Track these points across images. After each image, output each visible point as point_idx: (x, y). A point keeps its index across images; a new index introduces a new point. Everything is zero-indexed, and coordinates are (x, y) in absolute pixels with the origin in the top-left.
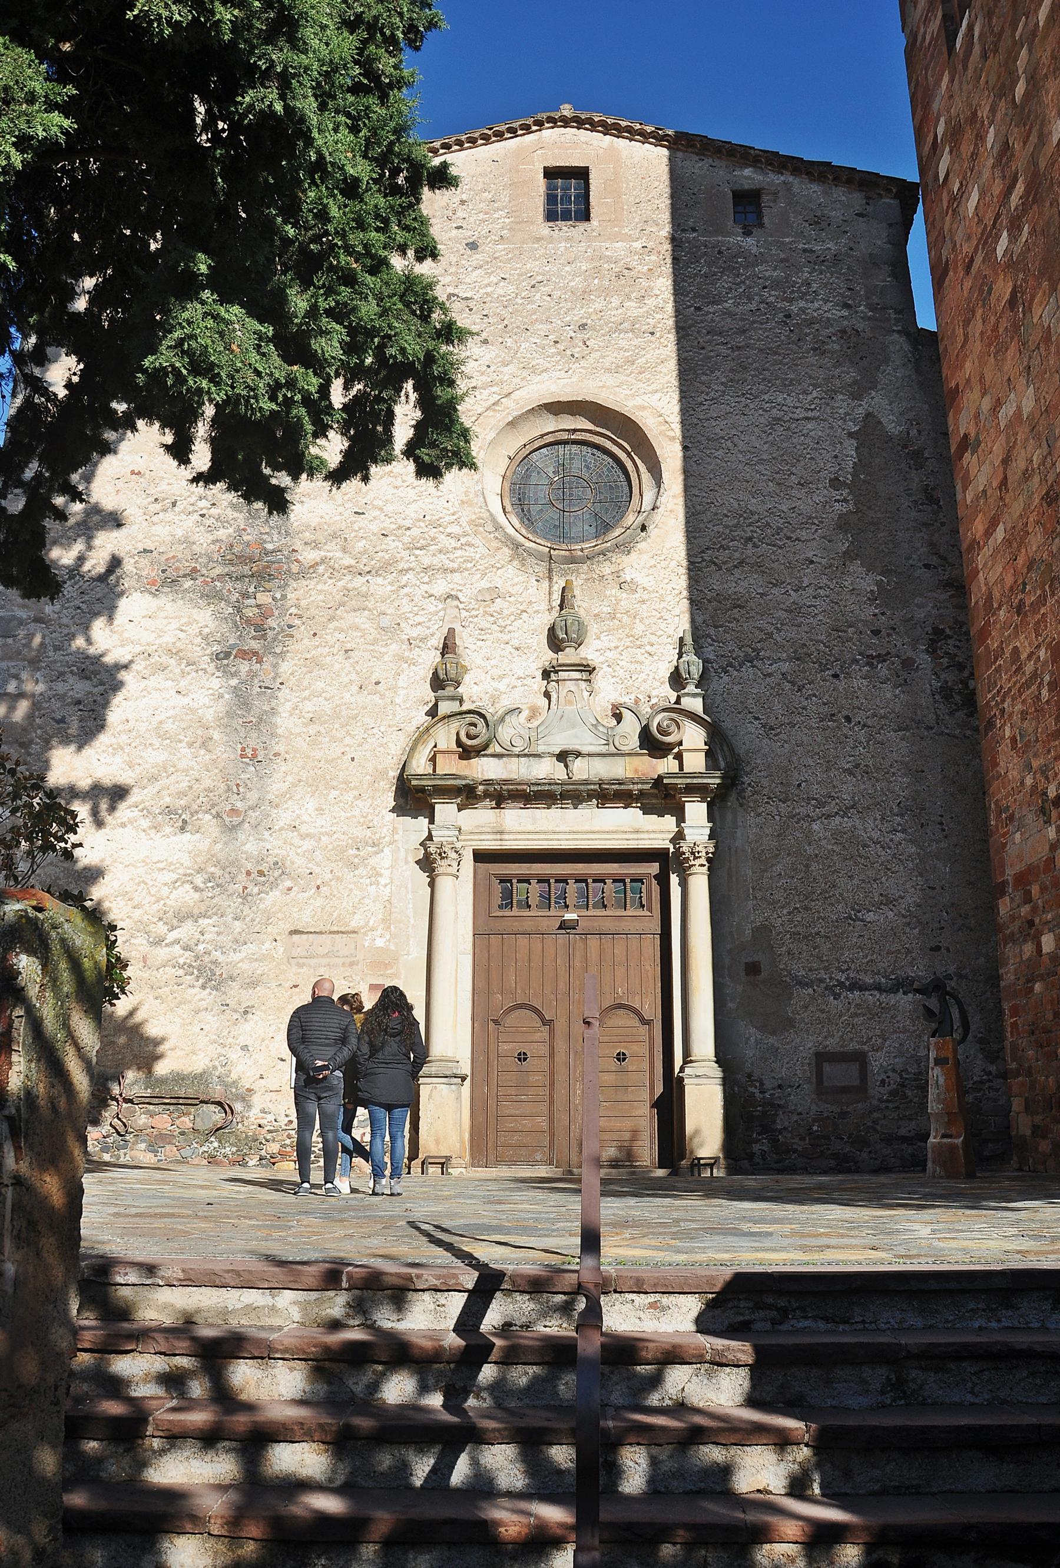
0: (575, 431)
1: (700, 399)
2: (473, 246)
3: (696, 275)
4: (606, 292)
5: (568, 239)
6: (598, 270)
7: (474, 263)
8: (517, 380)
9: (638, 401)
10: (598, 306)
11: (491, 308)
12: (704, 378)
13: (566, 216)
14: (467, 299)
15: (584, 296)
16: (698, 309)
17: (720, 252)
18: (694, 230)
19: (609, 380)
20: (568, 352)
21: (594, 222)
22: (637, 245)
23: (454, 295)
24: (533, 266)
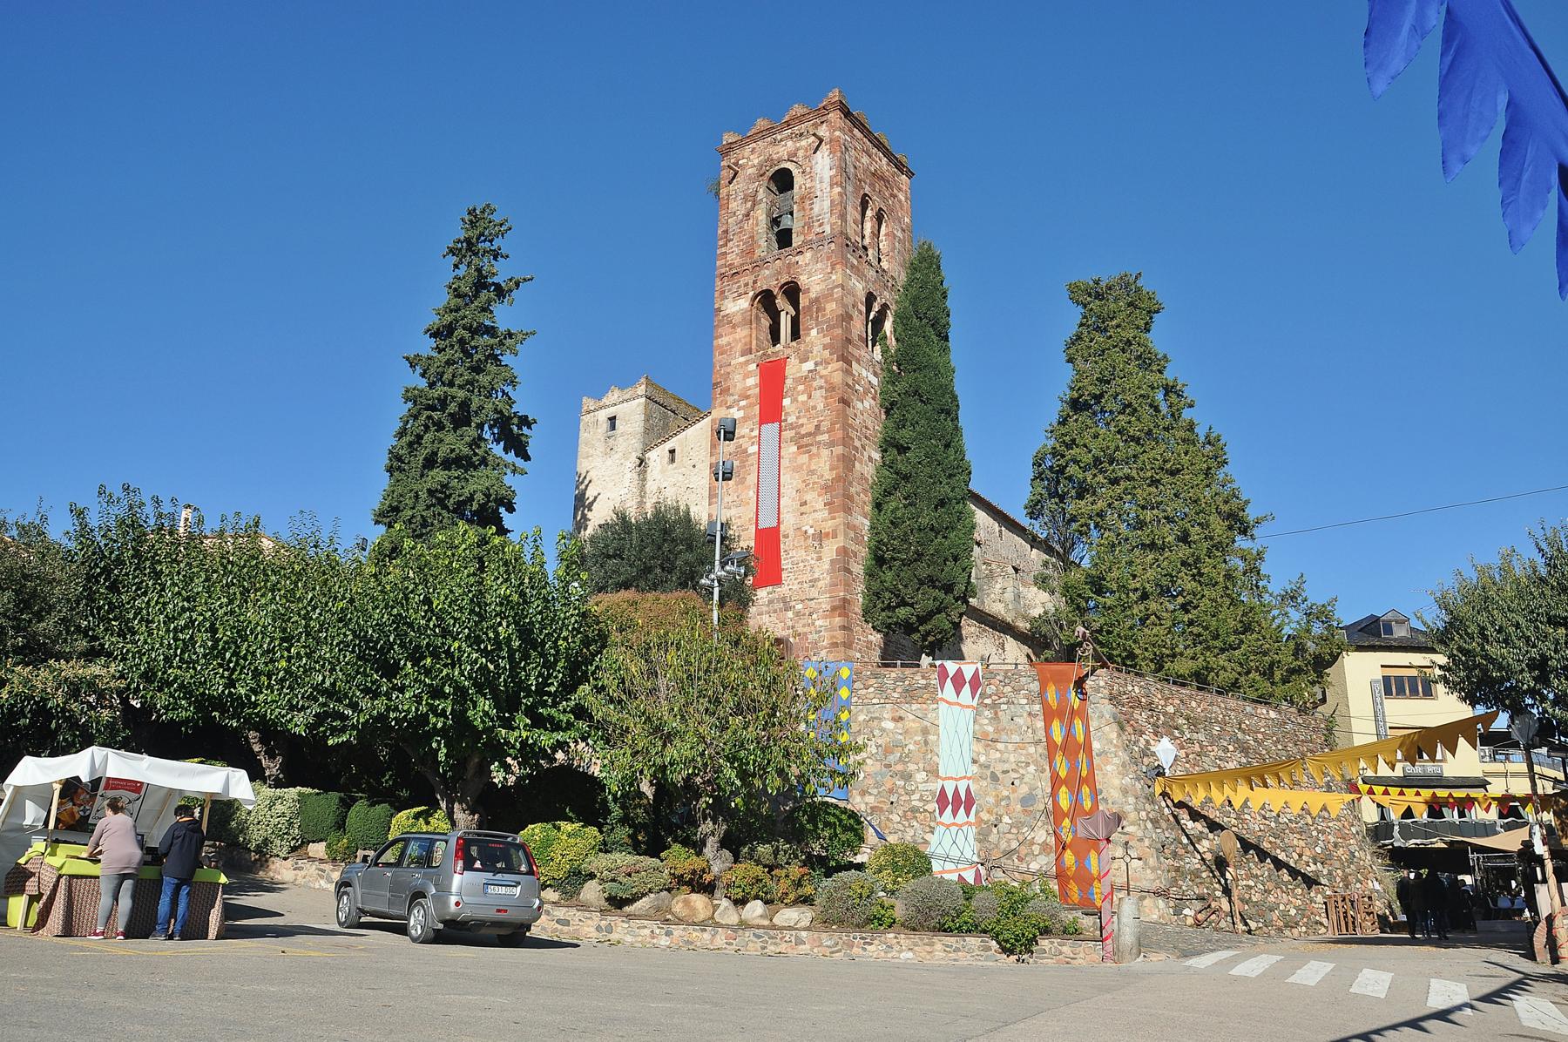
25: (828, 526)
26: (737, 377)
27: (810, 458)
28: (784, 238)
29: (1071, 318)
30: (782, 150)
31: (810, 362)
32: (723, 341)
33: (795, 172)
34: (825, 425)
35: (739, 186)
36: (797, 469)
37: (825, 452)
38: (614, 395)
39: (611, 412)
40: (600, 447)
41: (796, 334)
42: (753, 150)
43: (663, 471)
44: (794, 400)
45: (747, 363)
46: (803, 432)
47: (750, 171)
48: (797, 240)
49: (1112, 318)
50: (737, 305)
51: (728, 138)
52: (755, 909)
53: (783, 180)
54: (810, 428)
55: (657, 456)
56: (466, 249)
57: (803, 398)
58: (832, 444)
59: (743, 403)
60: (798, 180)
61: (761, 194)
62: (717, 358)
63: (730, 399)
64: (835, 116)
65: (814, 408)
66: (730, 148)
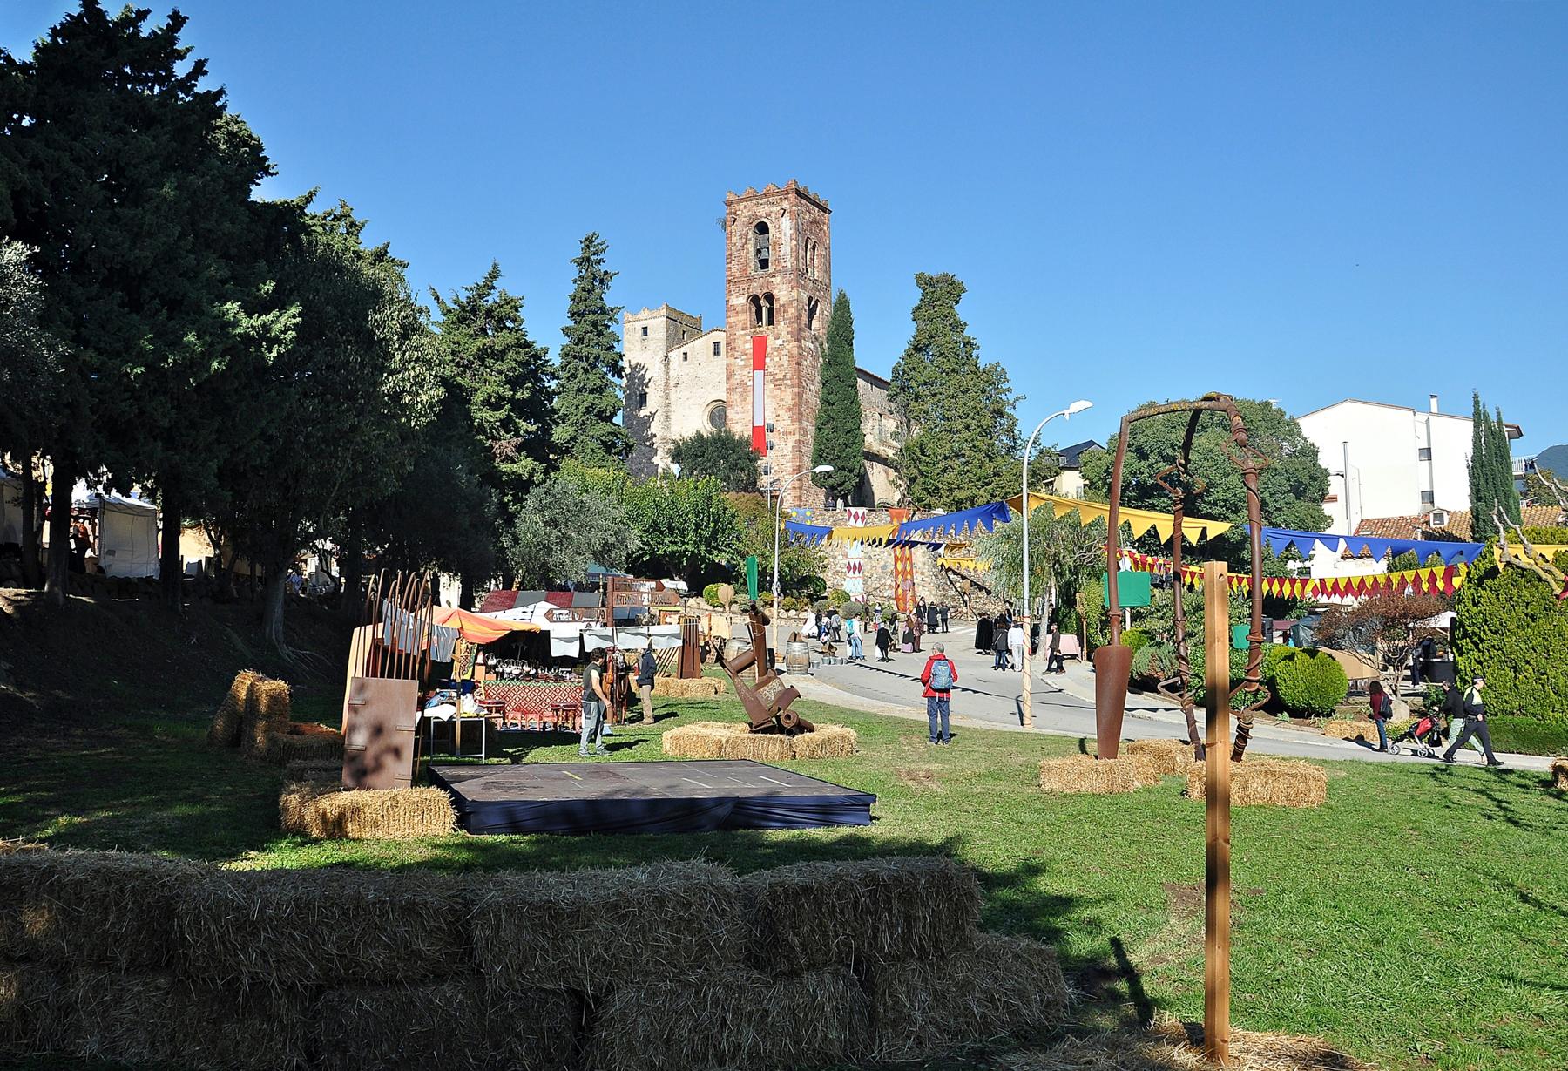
25: (791, 429)
26: (740, 342)
28: (764, 264)
29: (915, 296)
30: (763, 211)
31: (779, 338)
35: (737, 228)
36: (774, 397)
38: (644, 314)
39: (644, 323)
40: (638, 345)
41: (771, 322)
48: (771, 269)
49: (939, 295)
52: (792, 613)
53: (762, 229)
55: (676, 356)
56: (584, 262)
60: (772, 230)
61: (750, 235)
64: (792, 196)
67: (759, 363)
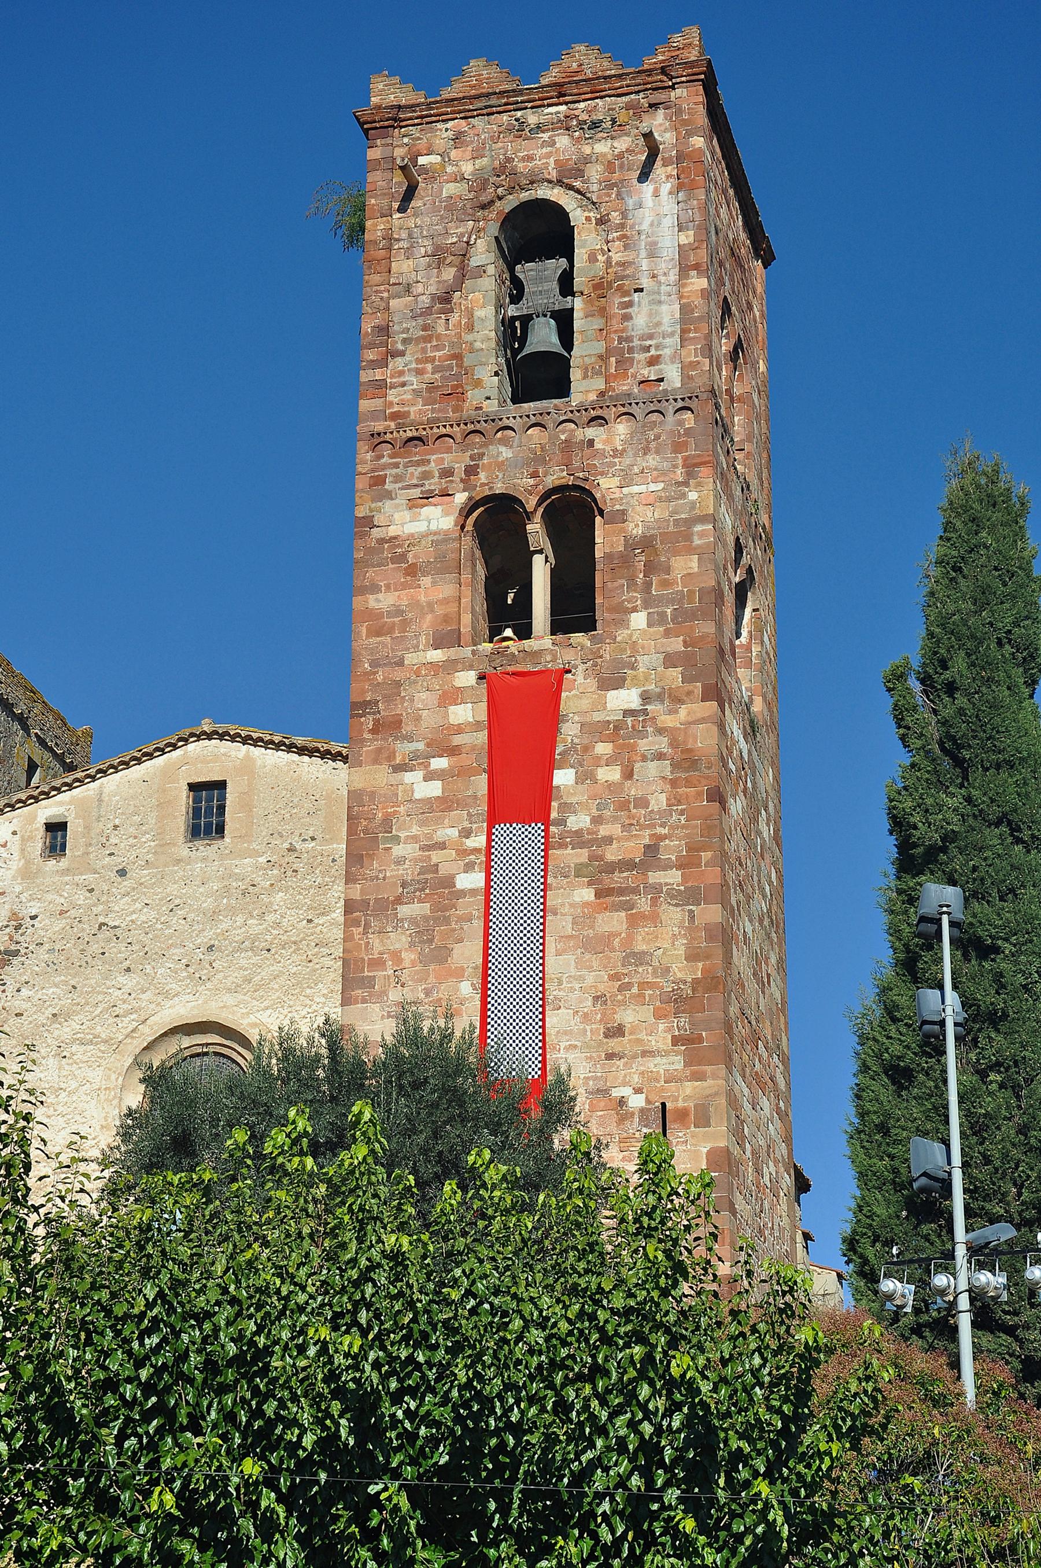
0: (208, 1044)
1: (304, 1013)
2: (122, 873)
3: (311, 887)
4: (232, 911)
5: (204, 859)
6: (227, 889)
7: (122, 891)
8: (153, 1006)
9: (252, 1019)
10: (224, 926)
11: (136, 935)
12: (308, 991)
13: (208, 832)
14: (115, 927)
15: (213, 916)
16: (310, 921)
17: (334, 860)
18: (313, 839)
19: (229, 999)
20: (197, 975)
21: (227, 840)
22: (262, 860)
23: (104, 924)
24: (172, 889)
25: (684, 1095)
26: (422, 698)
27: (634, 921)
30: (544, 152)
31: (622, 684)
32: (382, 601)
33: (577, 216)
34: (672, 849)
35: (421, 221)
36: (598, 945)
37: (673, 915)
42: (458, 139)
43: (27, 874)
44: (585, 777)
45: (451, 666)
46: (612, 854)
47: (450, 189)
48: (584, 388)
50: (425, 520)
51: (386, 92)
53: (537, 233)
54: (632, 848)
57: (610, 774)
58: (690, 896)
59: (440, 763)
60: (586, 240)
61: (484, 253)
62: (363, 640)
63: (403, 749)
64: (689, 98)
65: (642, 802)
66: (395, 118)
67: (518, 775)
